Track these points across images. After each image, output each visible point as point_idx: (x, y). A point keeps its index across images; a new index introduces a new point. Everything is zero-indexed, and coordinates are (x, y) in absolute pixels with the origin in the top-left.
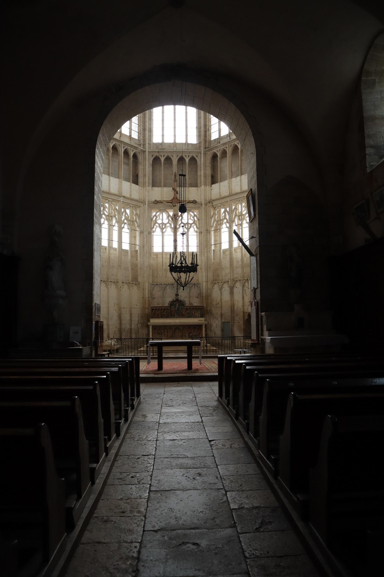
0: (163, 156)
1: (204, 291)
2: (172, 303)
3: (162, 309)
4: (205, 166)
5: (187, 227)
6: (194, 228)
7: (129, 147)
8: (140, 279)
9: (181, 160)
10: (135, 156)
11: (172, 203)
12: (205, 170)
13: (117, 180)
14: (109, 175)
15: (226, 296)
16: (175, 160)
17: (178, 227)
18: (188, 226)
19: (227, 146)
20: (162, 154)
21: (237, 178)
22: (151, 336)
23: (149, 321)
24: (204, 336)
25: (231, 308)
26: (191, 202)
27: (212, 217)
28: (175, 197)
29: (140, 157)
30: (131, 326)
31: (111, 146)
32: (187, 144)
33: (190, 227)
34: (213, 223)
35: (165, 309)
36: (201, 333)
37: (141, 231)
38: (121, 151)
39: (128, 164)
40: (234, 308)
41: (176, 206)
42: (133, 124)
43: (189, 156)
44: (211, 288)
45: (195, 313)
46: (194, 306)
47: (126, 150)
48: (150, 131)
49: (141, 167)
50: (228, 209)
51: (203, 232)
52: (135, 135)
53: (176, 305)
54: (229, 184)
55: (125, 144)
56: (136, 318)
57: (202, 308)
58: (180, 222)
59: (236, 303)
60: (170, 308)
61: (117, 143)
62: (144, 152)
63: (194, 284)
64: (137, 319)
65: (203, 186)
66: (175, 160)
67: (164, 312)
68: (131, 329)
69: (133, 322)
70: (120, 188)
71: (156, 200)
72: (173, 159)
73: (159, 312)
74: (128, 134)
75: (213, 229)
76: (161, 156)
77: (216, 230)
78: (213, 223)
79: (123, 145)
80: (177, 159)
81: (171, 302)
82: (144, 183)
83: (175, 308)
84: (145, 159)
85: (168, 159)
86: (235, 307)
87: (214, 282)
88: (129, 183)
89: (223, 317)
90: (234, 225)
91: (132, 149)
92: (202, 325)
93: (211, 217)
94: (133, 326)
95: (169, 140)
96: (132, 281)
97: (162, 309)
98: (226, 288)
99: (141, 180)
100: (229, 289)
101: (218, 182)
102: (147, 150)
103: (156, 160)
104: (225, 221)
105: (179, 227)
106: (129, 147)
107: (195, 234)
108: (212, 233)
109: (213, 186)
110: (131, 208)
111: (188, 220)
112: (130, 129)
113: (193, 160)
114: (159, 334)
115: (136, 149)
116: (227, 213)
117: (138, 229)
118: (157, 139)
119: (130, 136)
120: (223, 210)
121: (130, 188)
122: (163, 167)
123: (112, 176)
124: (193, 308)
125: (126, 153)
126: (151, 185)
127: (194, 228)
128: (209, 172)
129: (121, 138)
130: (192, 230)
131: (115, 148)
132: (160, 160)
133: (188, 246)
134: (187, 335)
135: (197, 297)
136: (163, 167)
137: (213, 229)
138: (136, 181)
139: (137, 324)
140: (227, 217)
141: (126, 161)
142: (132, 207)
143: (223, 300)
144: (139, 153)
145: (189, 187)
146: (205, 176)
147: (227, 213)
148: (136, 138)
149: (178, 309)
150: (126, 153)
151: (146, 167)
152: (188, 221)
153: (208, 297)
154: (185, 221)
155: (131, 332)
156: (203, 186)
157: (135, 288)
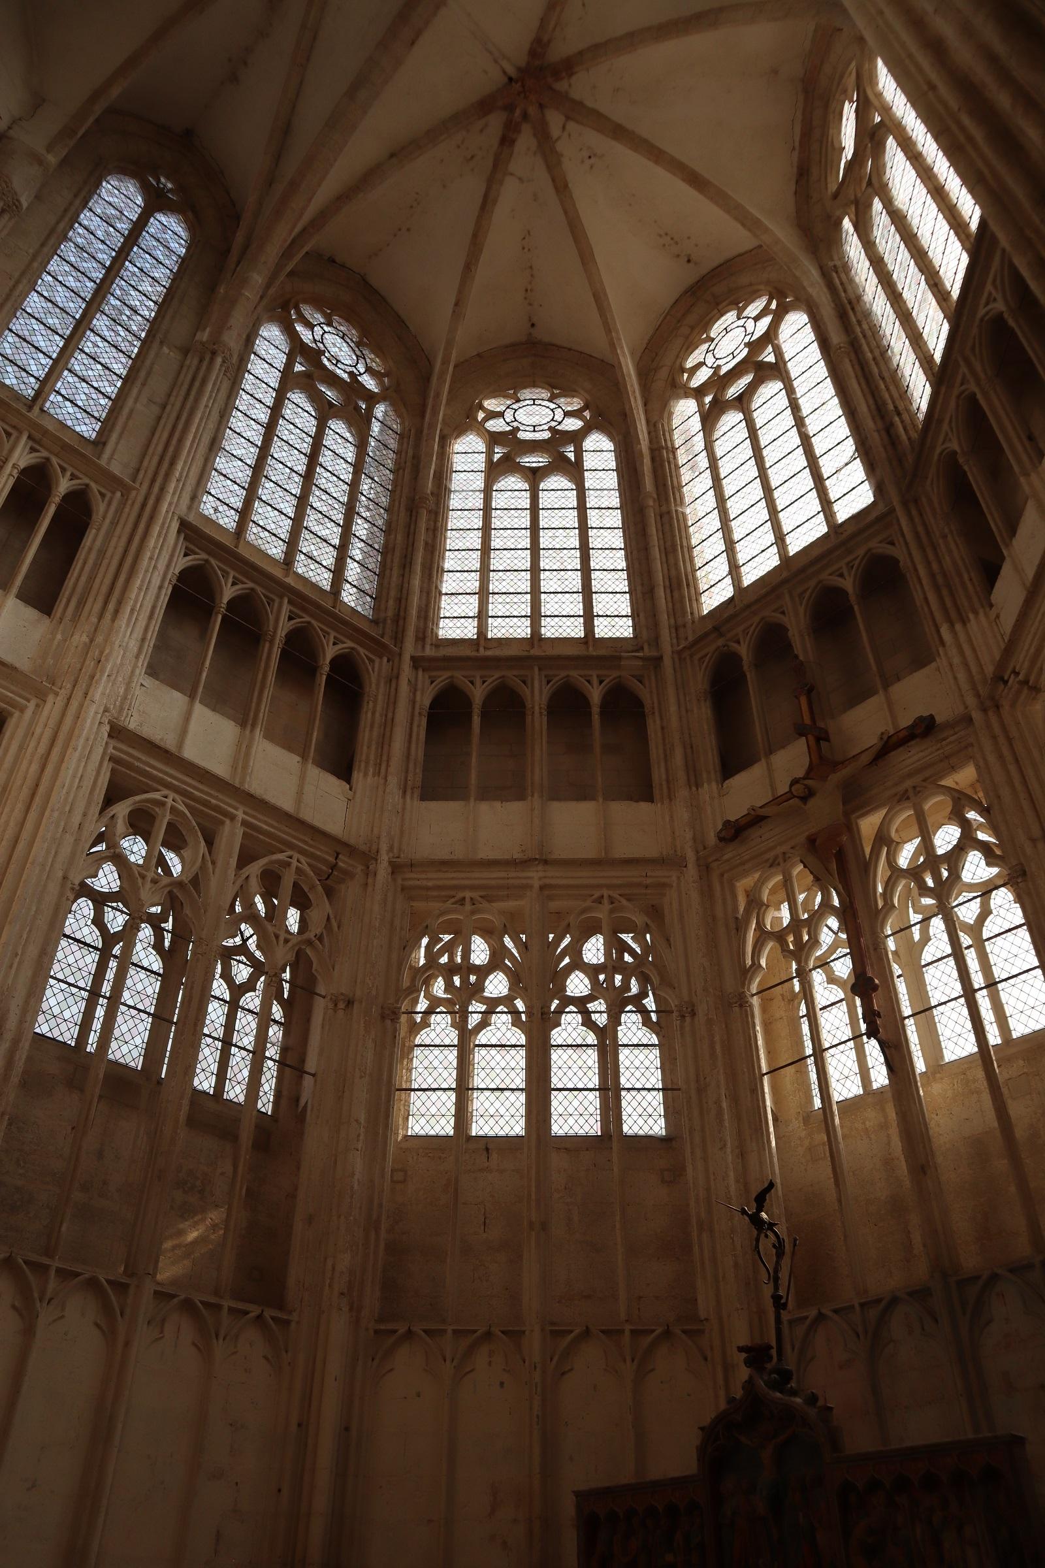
0: (478, 681)
14: (192, 697)
16: (537, 695)
43: (601, 682)
48: (431, 595)
66: (537, 695)
70: (242, 757)
87: (813, 1313)
95: (510, 625)
103: (446, 714)
113: (625, 707)
122: (476, 720)
126: (417, 793)
132: (467, 702)
136: (476, 720)
151: (397, 710)
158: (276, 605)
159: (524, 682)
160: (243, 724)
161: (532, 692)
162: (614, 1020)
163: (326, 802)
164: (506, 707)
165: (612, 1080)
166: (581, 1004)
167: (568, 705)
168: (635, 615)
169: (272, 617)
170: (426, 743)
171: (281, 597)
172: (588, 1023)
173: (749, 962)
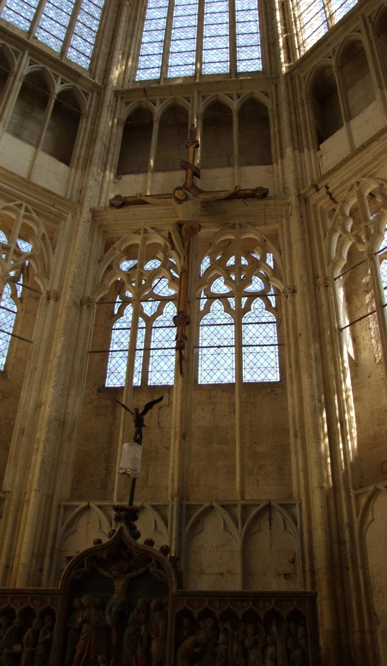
1: (319, 534)
4: (292, 103)
18: (238, 276)
19: (360, 23)
27: (334, 230)
29: (88, 105)
34: (339, 250)
35: (28, 614)
37: (48, 293)
41: (187, 198)
44: (356, 520)
45: (245, 654)
57: (297, 617)
60: (70, 610)
62: (100, 91)
63: (269, 507)
72: (188, 105)
75: (338, 272)
76: (155, 104)
85: (176, 117)
93: (329, 234)
106: (49, 69)
115: (75, 81)
121: (33, 161)
132: (150, 114)
135: (287, 576)
137: (338, 272)
145: (241, 165)
148: (84, 63)
158: (20, 55)
159: (189, 101)
161: (193, 106)
163: (51, 174)
165: (242, 348)
166: (223, 298)
168: (263, 58)
169: (17, 63)
172: (228, 309)
173: (334, 254)
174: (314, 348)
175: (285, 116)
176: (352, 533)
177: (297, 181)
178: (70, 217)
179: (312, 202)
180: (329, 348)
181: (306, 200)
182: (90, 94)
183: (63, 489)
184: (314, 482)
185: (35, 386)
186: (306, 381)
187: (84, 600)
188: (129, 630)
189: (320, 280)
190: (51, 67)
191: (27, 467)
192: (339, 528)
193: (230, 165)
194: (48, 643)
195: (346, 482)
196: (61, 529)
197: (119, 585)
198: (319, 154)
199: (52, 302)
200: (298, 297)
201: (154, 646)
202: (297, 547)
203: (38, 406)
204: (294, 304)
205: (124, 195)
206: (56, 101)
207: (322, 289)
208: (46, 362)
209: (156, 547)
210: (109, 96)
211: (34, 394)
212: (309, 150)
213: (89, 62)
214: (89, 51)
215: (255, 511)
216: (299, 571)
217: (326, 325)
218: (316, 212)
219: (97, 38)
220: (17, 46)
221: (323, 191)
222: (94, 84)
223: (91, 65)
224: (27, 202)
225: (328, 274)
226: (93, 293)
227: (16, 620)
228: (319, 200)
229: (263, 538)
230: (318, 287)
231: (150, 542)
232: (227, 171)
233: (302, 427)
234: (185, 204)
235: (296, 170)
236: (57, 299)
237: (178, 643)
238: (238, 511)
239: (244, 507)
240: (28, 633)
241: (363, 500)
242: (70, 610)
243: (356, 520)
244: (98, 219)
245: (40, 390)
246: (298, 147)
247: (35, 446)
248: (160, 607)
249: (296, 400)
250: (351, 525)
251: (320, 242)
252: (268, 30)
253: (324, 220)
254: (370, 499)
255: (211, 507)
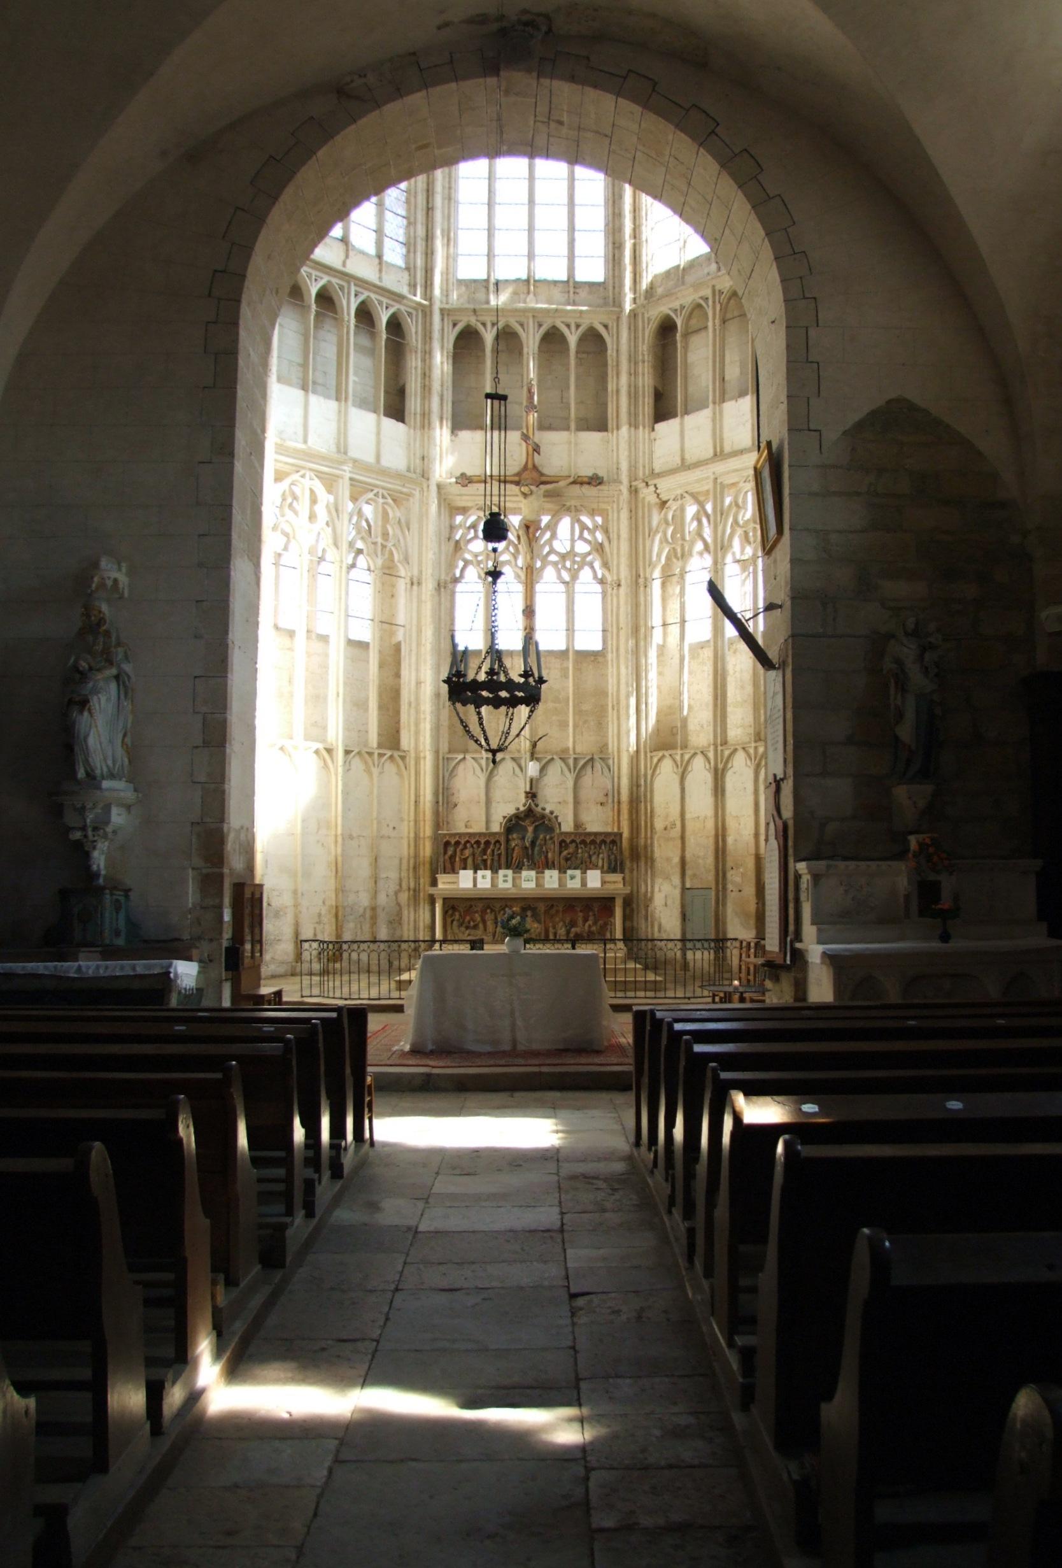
1: (625, 782)
2: (514, 824)
3: (478, 843)
4: (633, 360)
5: (568, 564)
6: (592, 568)
7: (373, 296)
8: (406, 741)
9: (552, 339)
10: (395, 326)
11: (517, 483)
12: (633, 374)
13: (333, 404)
14: (304, 388)
15: (700, 803)
16: (531, 341)
17: (539, 564)
18: (574, 562)
20: (488, 320)
21: (741, 401)
22: (439, 935)
23: (434, 883)
24: (619, 934)
25: (717, 842)
26: (582, 483)
27: (657, 531)
28: (530, 465)
29: (413, 329)
30: (375, 894)
31: (314, 291)
32: (571, 286)
33: (581, 568)
34: (659, 556)
36: (607, 925)
38: (349, 305)
39: (372, 352)
40: (724, 841)
42: (388, 216)
43: (578, 326)
44: (649, 772)
45: (590, 857)
46: (590, 834)
47: (363, 303)
49: (413, 363)
50: (709, 507)
51: (623, 583)
52: (395, 255)
53: (525, 829)
54: (714, 420)
55: (362, 283)
56: (391, 875)
57: (613, 842)
58: (547, 549)
59: (731, 824)
60: (508, 841)
61: (334, 281)
62: (426, 312)
63: (592, 759)
64: (394, 875)
65: (624, 430)
66: (531, 341)
67: (484, 852)
68: (374, 909)
69: (381, 884)
71: (463, 475)
73: (467, 852)
74: (372, 251)
77: (666, 578)
78: (659, 556)
79: (353, 288)
80: (538, 337)
81: (510, 820)
82: (426, 416)
83: (523, 838)
84: (427, 336)
86: (730, 840)
88: (371, 417)
89: (689, 873)
90: (729, 558)
91: (385, 301)
92: (611, 900)
93: (652, 533)
94: (382, 899)
95: (511, 268)
96: (380, 746)
97: (478, 843)
98: (700, 775)
99: (413, 404)
100: (709, 777)
101: (674, 416)
102: (437, 306)
103: (467, 342)
104: (699, 546)
105: (543, 568)
106: (373, 296)
107: (598, 588)
108: (656, 585)
109: (660, 426)
110: (381, 500)
111: (573, 541)
112: (380, 232)
113: (593, 340)
114: (467, 928)
116: (704, 520)
117: (402, 573)
118: (471, 268)
119: (380, 256)
120: (691, 510)
121: (378, 433)
123: (314, 392)
124: (583, 842)
125: (365, 315)
127: (592, 568)
128: (646, 380)
129: (348, 262)
130: (586, 574)
131: (326, 299)
133: (570, 630)
134: (562, 932)
138: (396, 409)
139: (396, 893)
140: (707, 533)
141: (365, 341)
142: (383, 497)
143: (688, 816)
144: (410, 314)
146: (633, 395)
147: (704, 520)
149: (533, 843)
150: (365, 315)
152: (573, 546)
153: (639, 800)
154: (562, 545)
155: (374, 918)
156: (624, 430)
157: (390, 768)
160: (338, 399)
162: (575, 577)
164: (508, 338)
167: (552, 339)
170: (454, 387)
171: (349, 283)
173: (654, 558)
174: (631, 643)
175: (624, 379)
176: (645, 781)
177: (630, 470)
178: (417, 494)
179: (641, 496)
180: (642, 643)
181: (636, 491)
182: (414, 313)
183: (444, 747)
184: (624, 746)
185: (413, 667)
186: (623, 670)
187: (515, 836)
188: (537, 849)
189: (641, 581)
190: (374, 292)
191: (417, 733)
192: (638, 776)
193: (568, 429)
194: (499, 855)
195: (645, 747)
196: (447, 775)
197: (530, 829)
198: (653, 435)
199: (415, 587)
200: (622, 590)
201: (550, 855)
202: (610, 787)
203: (419, 683)
204: (618, 596)
205: (469, 473)
206: (388, 339)
207: (642, 589)
208: (419, 644)
209: (547, 811)
210: (437, 318)
211: (413, 674)
212: (644, 427)
213: (404, 251)
214: (401, 232)
215: (582, 763)
216: (610, 801)
217: (642, 623)
218: (643, 507)
219: (408, 202)
220: (340, 279)
221: (652, 488)
222: (420, 304)
223: (407, 257)
224: (383, 488)
225: (648, 575)
226: (447, 574)
227: (482, 846)
228: (647, 495)
229: (587, 779)
230: (639, 583)
231: (544, 809)
232: (564, 435)
233: (618, 703)
234: (531, 498)
235: (630, 456)
236: (419, 584)
237: (560, 853)
238: (571, 762)
239: (575, 759)
240: (489, 851)
241: (655, 760)
242: (508, 841)
243: (649, 772)
244: (443, 492)
245: (417, 670)
246: (634, 424)
247: (422, 716)
248: (551, 838)
249: (615, 682)
250: (645, 775)
251: (644, 539)
252: (614, 213)
253: (650, 516)
254: (659, 760)
255: (552, 759)
